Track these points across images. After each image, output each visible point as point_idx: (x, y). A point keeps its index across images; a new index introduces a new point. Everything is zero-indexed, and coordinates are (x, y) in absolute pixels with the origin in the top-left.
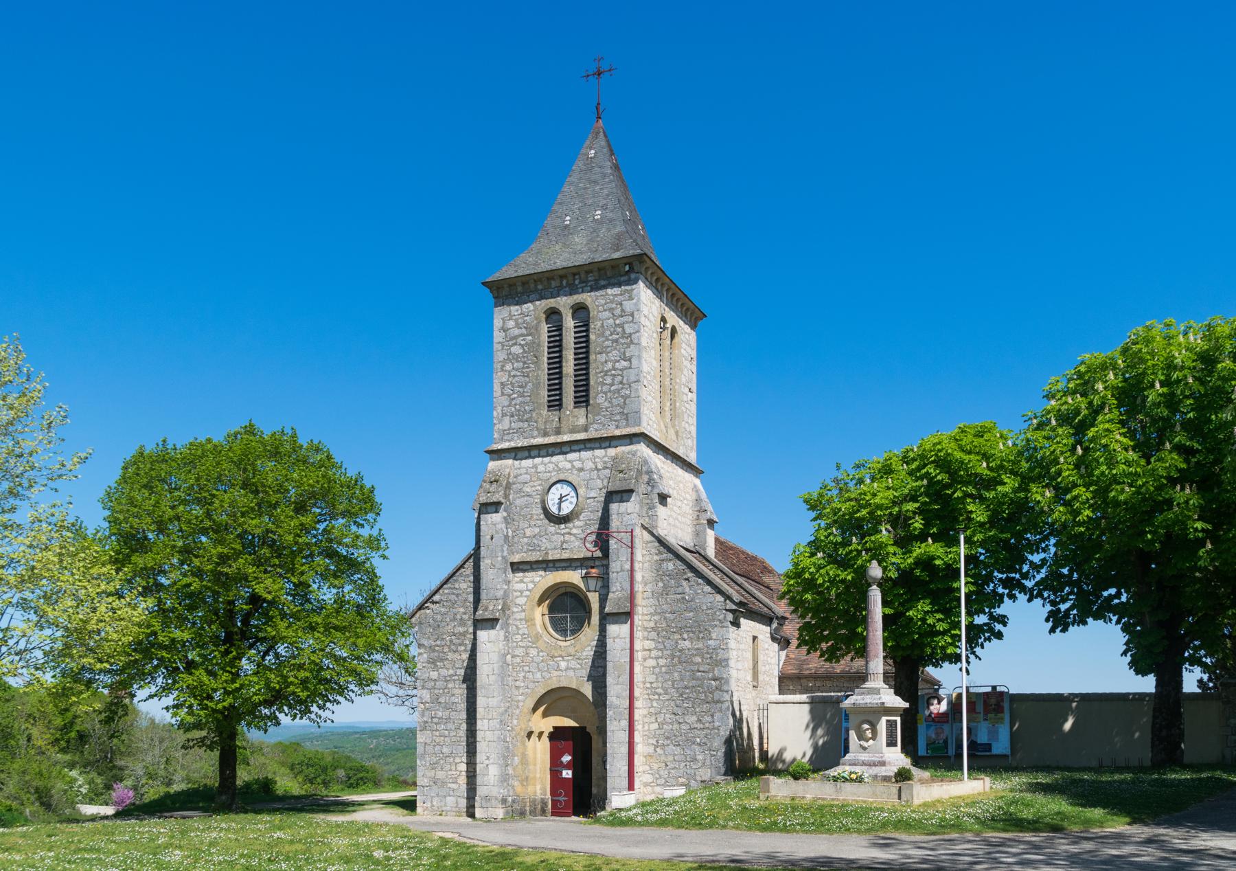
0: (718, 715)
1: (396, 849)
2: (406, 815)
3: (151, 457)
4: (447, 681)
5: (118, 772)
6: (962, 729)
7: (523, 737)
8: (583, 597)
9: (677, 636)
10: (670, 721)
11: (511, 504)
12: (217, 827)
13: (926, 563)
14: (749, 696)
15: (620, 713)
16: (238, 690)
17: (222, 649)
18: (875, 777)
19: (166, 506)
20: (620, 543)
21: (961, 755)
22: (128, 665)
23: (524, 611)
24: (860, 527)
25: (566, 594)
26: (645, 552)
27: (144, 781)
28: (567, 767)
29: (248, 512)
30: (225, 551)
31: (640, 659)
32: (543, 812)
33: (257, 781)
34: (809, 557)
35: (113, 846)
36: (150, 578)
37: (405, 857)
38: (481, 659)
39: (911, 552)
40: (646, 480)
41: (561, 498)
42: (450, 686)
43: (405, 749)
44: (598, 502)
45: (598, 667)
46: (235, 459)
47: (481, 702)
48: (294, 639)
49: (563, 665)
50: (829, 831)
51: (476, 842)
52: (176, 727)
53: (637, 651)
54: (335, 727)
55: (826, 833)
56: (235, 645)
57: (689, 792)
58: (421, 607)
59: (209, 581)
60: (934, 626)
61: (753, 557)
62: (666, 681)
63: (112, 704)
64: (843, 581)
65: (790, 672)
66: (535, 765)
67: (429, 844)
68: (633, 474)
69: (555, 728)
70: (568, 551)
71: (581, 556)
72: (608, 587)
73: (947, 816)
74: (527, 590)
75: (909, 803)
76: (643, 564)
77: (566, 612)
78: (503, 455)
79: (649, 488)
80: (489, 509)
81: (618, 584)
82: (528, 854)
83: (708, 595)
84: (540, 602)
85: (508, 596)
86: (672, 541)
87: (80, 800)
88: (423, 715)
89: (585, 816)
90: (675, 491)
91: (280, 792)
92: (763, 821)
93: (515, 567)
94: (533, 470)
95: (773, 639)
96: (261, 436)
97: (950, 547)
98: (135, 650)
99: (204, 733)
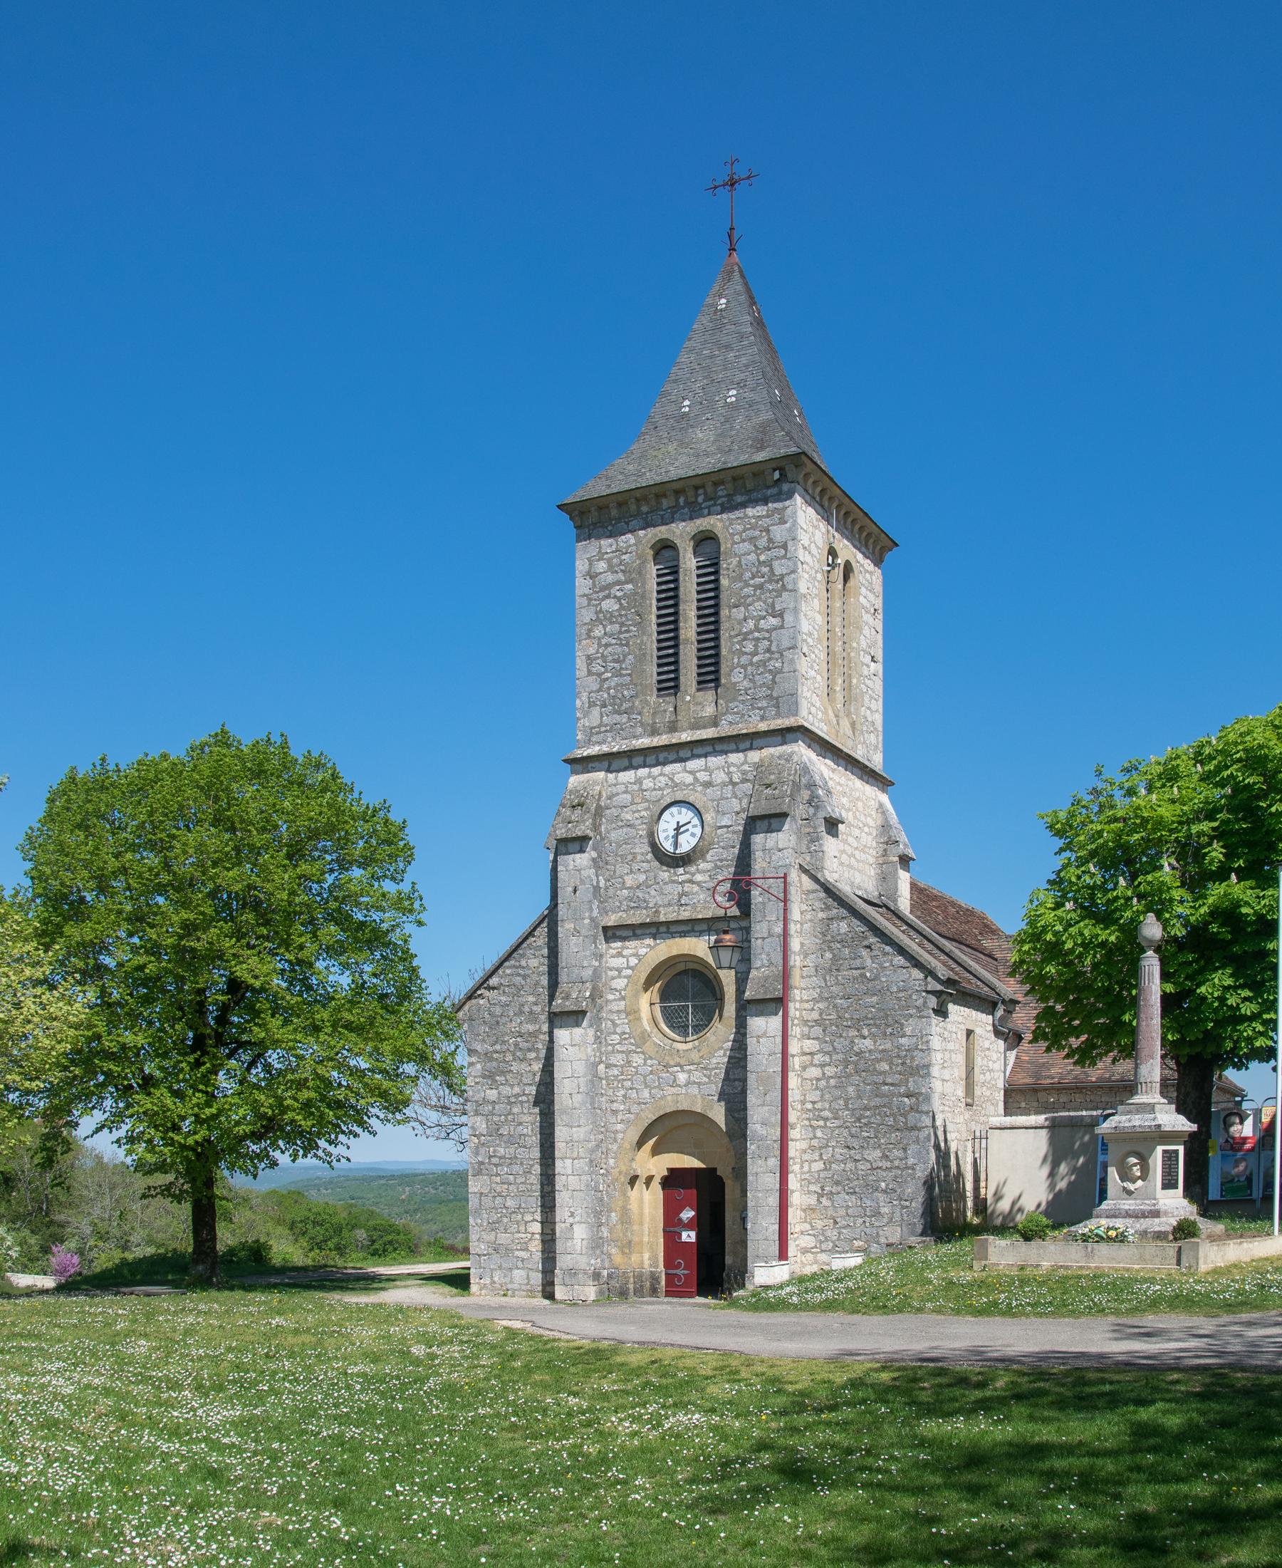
0: (913, 1148)
1: (443, 1343)
2: (455, 1295)
3: (86, 783)
4: (510, 1103)
5: (58, 1230)
6: (1273, 1160)
7: (623, 1184)
8: (711, 977)
9: (853, 1033)
10: (841, 1158)
11: (603, 839)
12: (194, 1309)
13: (1228, 914)
14: (960, 1119)
15: (768, 1148)
16: (214, 1117)
17: (191, 1059)
18: (1143, 1234)
19: (108, 854)
20: (767, 895)
21: (1271, 1198)
22: (70, 1082)
23: (623, 998)
24: (1129, 862)
25: (685, 972)
26: (804, 907)
27: (91, 1243)
28: (688, 1226)
29: (220, 859)
30: (192, 916)
31: (797, 1067)
32: (654, 1291)
33: (243, 1246)
34: (1054, 909)
35: (57, 1331)
36: (89, 958)
37: (456, 1355)
38: (561, 1071)
39: (1205, 897)
40: (807, 797)
41: (677, 829)
42: (515, 1110)
43: (451, 1201)
44: (734, 832)
45: (735, 1080)
46: (202, 783)
47: (561, 1133)
48: (291, 1044)
49: (682, 1077)
50: (1074, 1314)
51: (557, 1335)
52: (132, 1169)
53: (793, 1056)
54: (350, 1169)
55: (1069, 1316)
56: (208, 1053)
57: (869, 1261)
58: (471, 996)
59: (169, 961)
60: (1238, 1008)
61: (968, 910)
62: (836, 1099)
63: (47, 1137)
64: (1103, 944)
65: (1021, 1081)
66: (641, 1224)
67: (490, 1337)
68: (787, 788)
69: (671, 1170)
70: (689, 908)
71: (709, 915)
72: (749, 960)
73: (1247, 1287)
74: (628, 968)
75: (1192, 1270)
76: (802, 924)
77: (686, 1000)
78: (590, 765)
79: (811, 811)
80: (571, 846)
81: (764, 956)
82: (633, 1352)
83: (899, 971)
84: (648, 985)
85: (600, 977)
86: (845, 889)
87: (10, 1267)
88: (477, 1154)
89: (715, 1296)
90: (850, 813)
91: (277, 1261)
92: (977, 1301)
93: (610, 933)
94: (636, 787)
95: (998, 1033)
96: (238, 748)
97: (1263, 890)
98: (73, 1061)
99: (170, 1177)
